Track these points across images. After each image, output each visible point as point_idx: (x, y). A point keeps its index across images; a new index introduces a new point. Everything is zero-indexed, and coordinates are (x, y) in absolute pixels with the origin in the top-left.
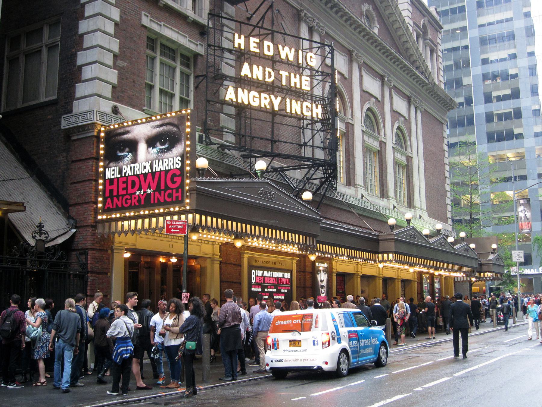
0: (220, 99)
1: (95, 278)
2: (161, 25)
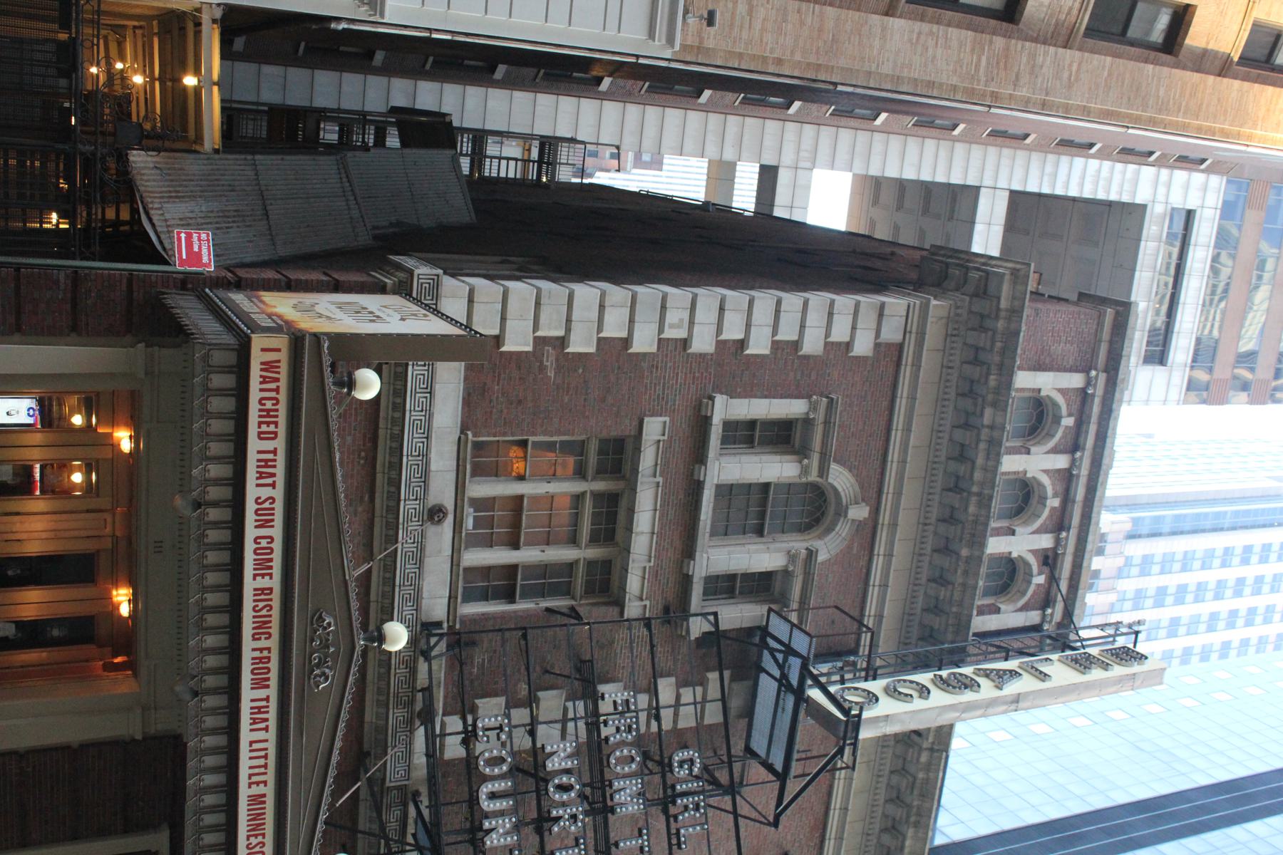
0: (540, 694)
1: (62, 287)
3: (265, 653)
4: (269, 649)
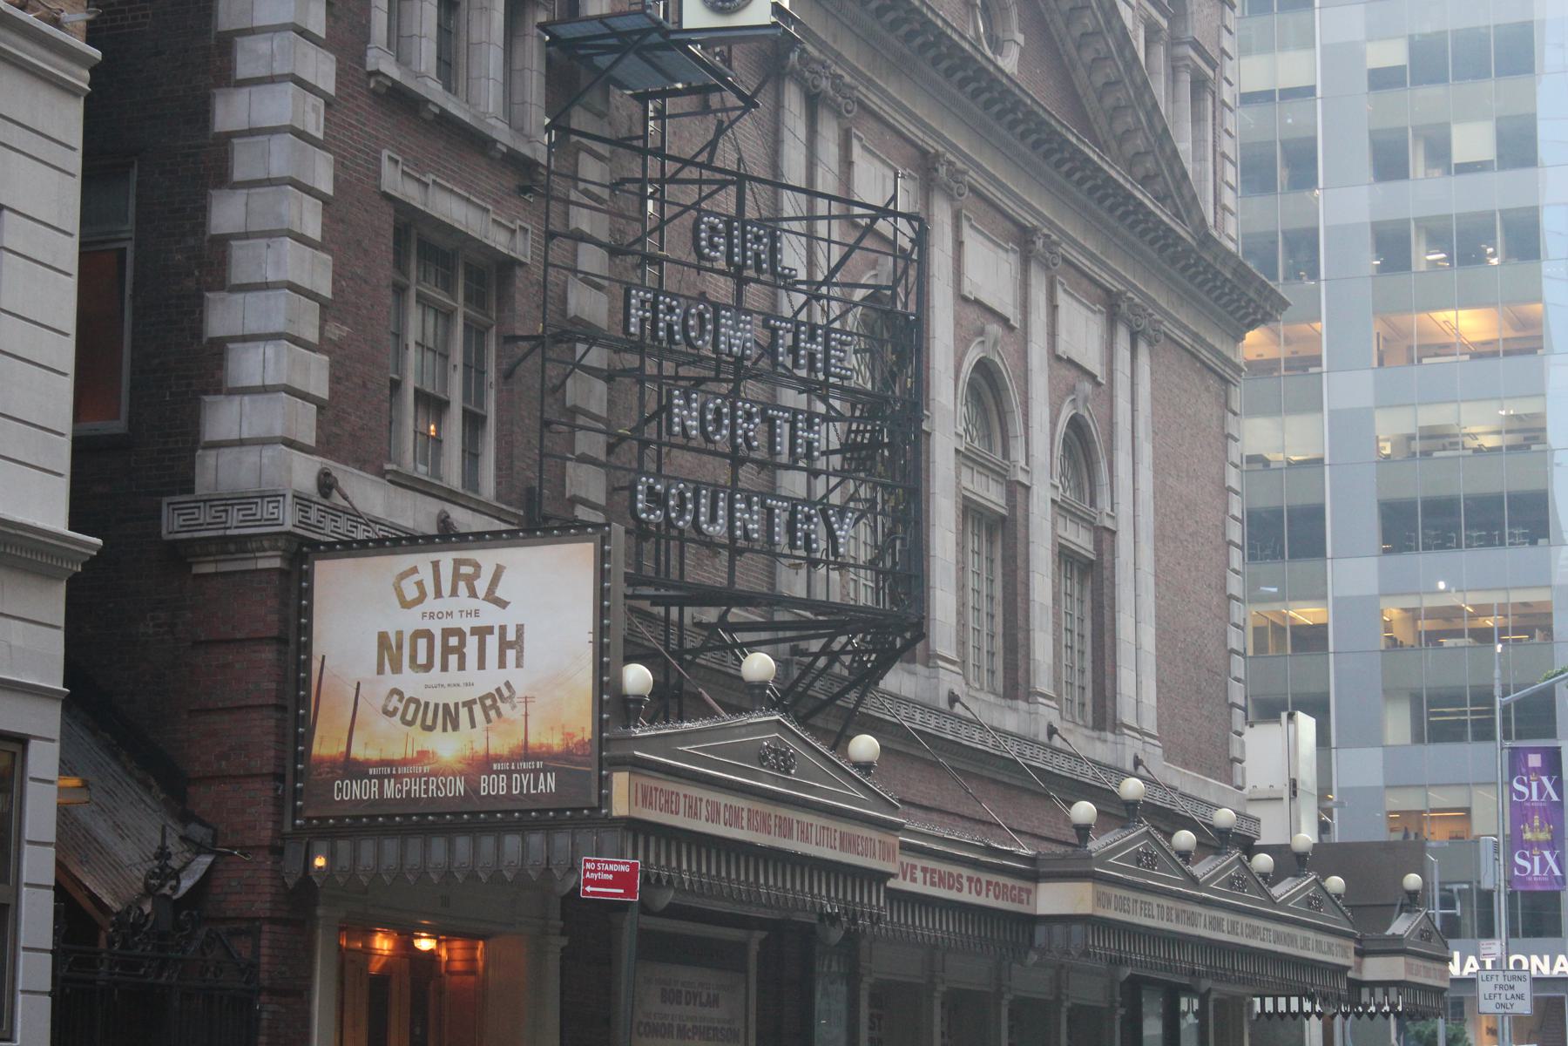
2: (426, 185)
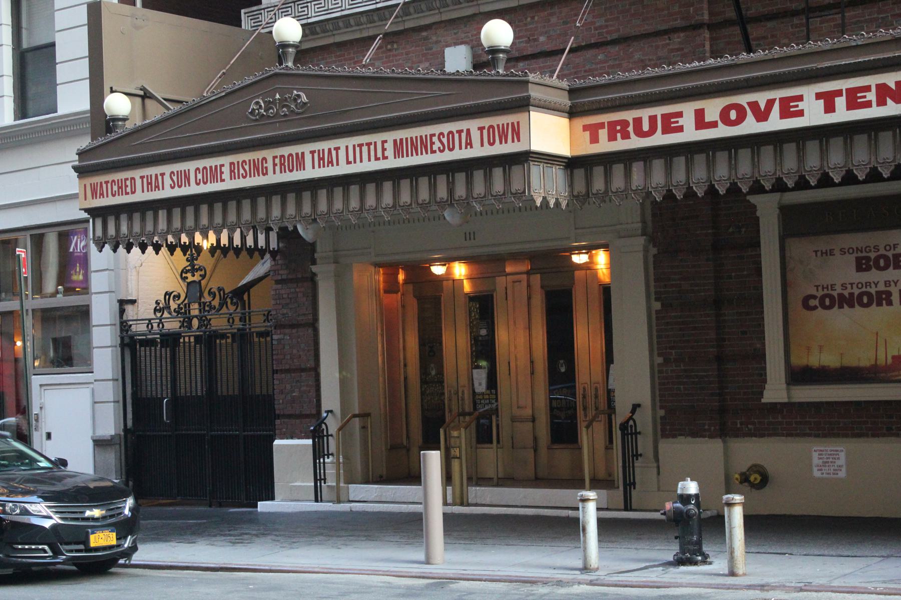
3: (277, 161)
4: (275, 158)
